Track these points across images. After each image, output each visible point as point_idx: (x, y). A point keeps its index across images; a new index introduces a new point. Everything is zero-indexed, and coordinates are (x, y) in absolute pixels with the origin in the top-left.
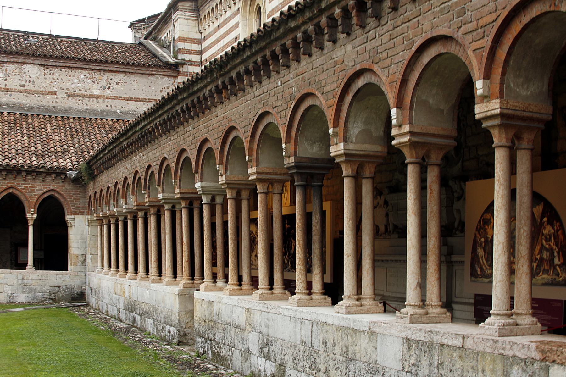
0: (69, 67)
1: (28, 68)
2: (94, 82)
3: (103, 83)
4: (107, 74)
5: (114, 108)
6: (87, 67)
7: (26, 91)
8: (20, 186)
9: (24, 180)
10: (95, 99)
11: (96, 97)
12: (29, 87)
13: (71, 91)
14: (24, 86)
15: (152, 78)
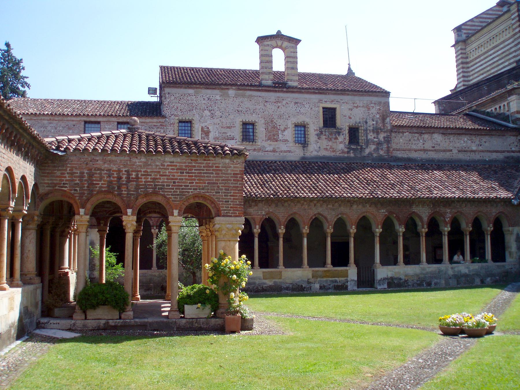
0: (459, 134)
1: (436, 136)
2: (472, 142)
3: (478, 142)
4: (479, 137)
5: (485, 158)
6: (469, 133)
7: (435, 150)
9: (486, 207)
10: (474, 153)
11: (474, 151)
12: (437, 148)
13: (460, 149)
14: (434, 147)
15: (504, 138)
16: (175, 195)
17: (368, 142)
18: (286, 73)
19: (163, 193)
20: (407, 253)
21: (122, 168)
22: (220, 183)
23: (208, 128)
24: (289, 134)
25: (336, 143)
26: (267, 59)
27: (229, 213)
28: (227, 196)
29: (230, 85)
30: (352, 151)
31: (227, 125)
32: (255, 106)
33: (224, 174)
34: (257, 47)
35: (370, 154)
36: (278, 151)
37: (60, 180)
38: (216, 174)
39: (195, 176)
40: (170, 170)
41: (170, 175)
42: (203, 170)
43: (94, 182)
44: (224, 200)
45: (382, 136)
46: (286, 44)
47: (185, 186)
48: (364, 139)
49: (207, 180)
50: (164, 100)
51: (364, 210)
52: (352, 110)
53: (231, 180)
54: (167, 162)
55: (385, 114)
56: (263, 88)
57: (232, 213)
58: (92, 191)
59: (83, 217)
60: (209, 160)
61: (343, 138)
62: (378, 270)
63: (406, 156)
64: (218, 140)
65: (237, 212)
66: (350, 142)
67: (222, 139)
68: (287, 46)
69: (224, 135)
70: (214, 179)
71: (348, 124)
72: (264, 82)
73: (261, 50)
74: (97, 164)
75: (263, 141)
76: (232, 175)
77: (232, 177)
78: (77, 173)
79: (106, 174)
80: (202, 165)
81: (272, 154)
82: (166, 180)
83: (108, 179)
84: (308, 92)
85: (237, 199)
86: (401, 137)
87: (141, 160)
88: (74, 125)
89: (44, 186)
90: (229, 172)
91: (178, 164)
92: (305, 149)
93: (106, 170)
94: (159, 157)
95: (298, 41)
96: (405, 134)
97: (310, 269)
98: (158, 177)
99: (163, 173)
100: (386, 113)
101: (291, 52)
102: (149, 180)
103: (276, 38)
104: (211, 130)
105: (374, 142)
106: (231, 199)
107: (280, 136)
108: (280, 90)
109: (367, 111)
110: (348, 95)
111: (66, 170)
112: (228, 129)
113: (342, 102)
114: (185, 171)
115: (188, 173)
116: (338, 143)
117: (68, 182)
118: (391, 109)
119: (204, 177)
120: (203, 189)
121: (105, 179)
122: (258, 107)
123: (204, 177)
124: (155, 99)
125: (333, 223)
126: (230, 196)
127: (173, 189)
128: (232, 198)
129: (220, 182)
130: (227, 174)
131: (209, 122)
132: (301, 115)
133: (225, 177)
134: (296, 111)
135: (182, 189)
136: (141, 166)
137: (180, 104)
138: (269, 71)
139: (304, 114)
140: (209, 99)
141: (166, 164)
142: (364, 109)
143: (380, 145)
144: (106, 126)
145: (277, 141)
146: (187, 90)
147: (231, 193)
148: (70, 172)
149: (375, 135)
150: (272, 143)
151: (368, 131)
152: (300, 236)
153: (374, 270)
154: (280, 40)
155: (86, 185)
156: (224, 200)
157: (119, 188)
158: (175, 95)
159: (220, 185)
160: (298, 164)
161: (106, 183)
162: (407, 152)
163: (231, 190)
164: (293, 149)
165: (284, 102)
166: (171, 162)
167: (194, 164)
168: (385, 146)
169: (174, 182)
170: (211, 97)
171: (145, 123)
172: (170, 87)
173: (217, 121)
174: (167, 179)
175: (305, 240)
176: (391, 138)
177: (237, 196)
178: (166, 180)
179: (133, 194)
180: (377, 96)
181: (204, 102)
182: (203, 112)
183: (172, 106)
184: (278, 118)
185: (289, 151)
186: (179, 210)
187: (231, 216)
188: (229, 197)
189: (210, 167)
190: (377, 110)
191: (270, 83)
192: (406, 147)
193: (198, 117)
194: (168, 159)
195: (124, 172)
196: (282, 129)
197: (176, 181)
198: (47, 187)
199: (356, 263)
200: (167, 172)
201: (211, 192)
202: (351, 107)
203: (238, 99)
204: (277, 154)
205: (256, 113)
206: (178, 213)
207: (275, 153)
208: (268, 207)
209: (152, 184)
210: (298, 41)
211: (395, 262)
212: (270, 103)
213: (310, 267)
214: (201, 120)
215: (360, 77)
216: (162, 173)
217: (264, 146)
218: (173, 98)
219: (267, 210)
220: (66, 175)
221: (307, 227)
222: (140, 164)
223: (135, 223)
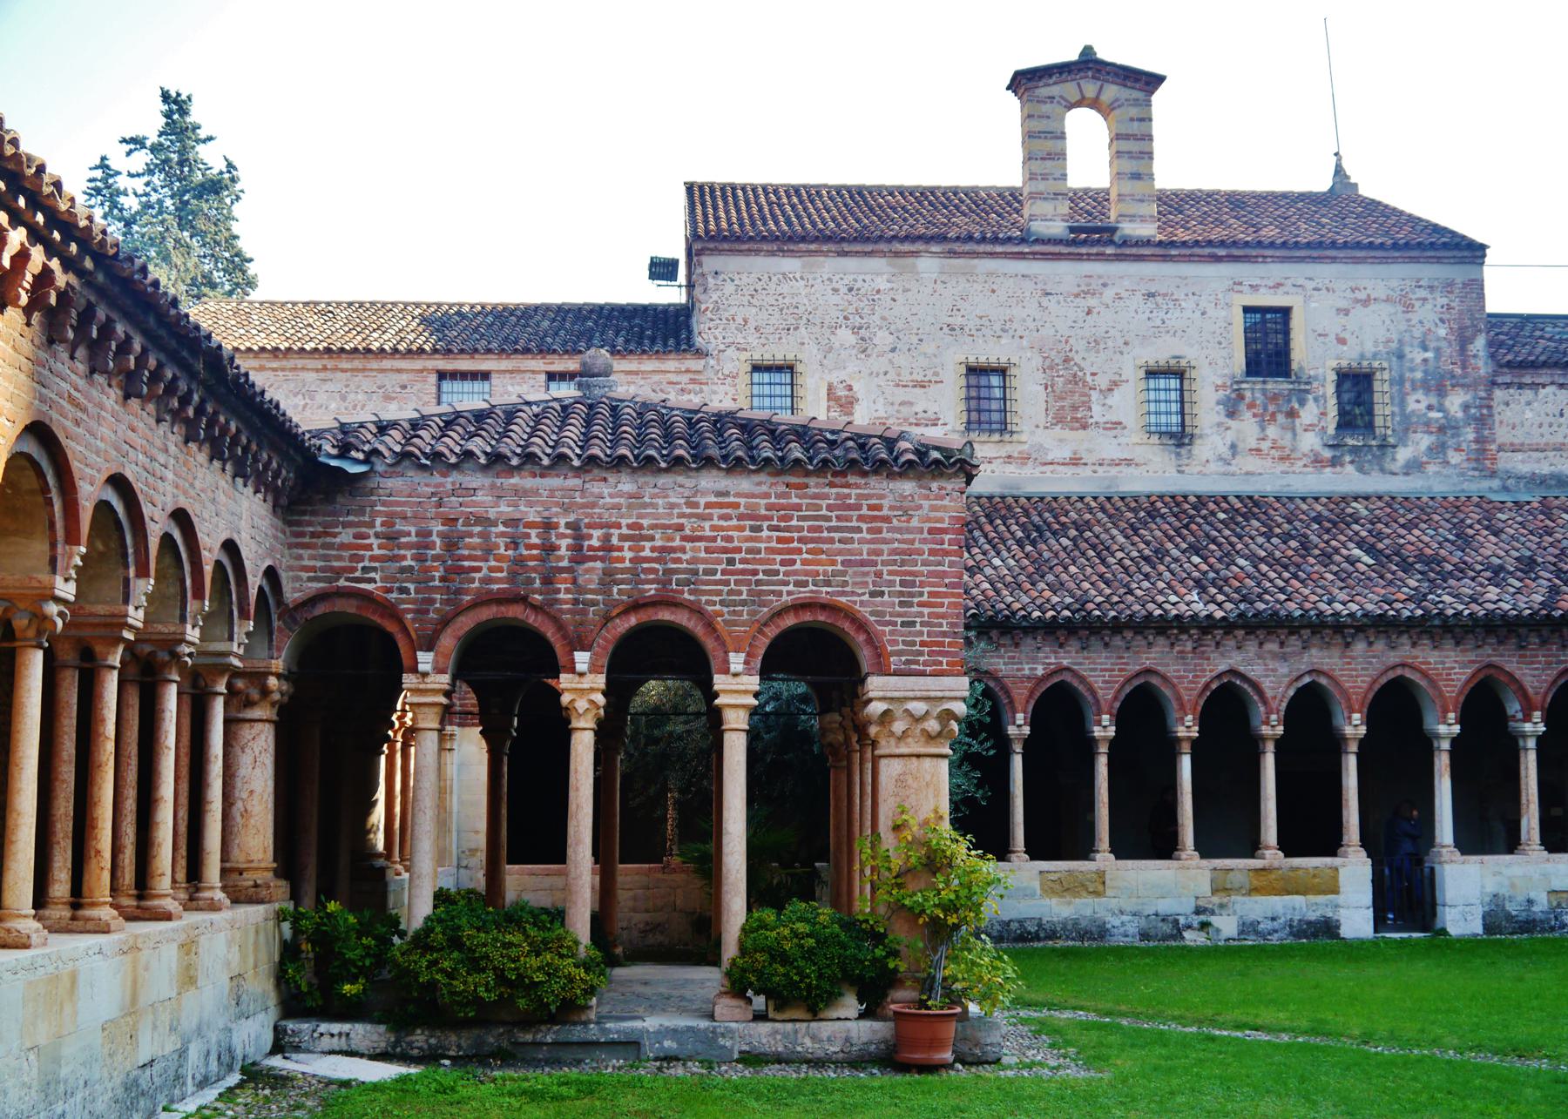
16: (734, 603)
17: (1407, 425)
18: (1113, 196)
19: (692, 598)
20: (1556, 812)
21: (557, 515)
22: (884, 563)
23: (850, 388)
24: (1127, 404)
25: (1293, 430)
26: (1049, 145)
27: (917, 663)
28: (911, 605)
29: (920, 238)
30: (1348, 458)
31: (915, 377)
32: (1008, 311)
33: (899, 530)
34: (1013, 103)
35: (1415, 466)
36: (1090, 461)
37: (352, 556)
38: (870, 531)
39: (800, 540)
40: (716, 522)
41: (715, 537)
42: (828, 519)
43: (466, 564)
44: (899, 620)
45: (1455, 402)
46: (1111, 92)
47: (765, 572)
48: (1393, 414)
49: (840, 553)
50: (702, 297)
51: (1393, 657)
52: (1346, 312)
53: (920, 552)
54: (704, 494)
55: (1468, 323)
56: (1037, 248)
57: (925, 663)
58: (458, 592)
59: (428, 680)
60: (848, 486)
61: (1316, 411)
62: (1447, 867)
63: (1545, 469)
65: (945, 660)
66: (1346, 423)
68: (1117, 100)
70: (865, 547)
71: (1334, 364)
72: (1039, 228)
73: (1028, 117)
74: (475, 504)
75: (1037, 426)
76: (925, 535)
77: (924, 541)
78: (409, 534)
79: (503, 534)
80: (824, 503)
81: (1070, 470)
82: (703, 555)
83: (510, 552)
84: (1190, 255)
85: (943, 616)
86: (1529, 403)
87: (620, 487)
88: (404, 387)
89: (298, 579)
90: (915, 523)
91: (742, 501)
92: (1183, 451)
93: (505, 524)
94: (681, 479)
95: (1152, 81)
96: (1542, 392)
97: (1205, 862)
98: (677, 543)
99: (693, 530)
100: (1472, 318)
101: (1132, 120)
102: (647, 553)
103: (1080, 70)
104: (859, 395)
105: (1428, 424)
106: (921, 614)
107: (1096, 409)
108: (1094, 250)
109: (1400, 316)
110: (1334, 260)
111: (371, 525)
112: (918, 391)
113: (1310, 285)
114: (765, 524)
115: (776, 528)
116: (1299, 430)
117: (377, 564)
118: (1493, 306)
119: (831, 541)
120: (828, 583)
121: (502, 551)
122: (1017, 312)
123: (831, 541)
124: (670, 294)
125: (1284, 705)
126: (920, 604)
127: (727, 583)
128: (926, 610)
129: (885, 558)
130: (908, 531)
131: (850, 369)
132: (1167, 337)
133: (900, 542)
134: (1151, 324)
135: (758, 583)
136: (618, 507)
137: (754, 310)
138: (1058, 187)
139: (1179, 333)
140: (851, 290)
141: (702, 501)
142: (1389, 308)
143: (1450, 433)
144: (510, 388)
145: (1084, 427)
146: (775, 259)
147: (921, 594)
148: (384, 529)
149: (1433, 400)
150: (1067, 434)
151: (1408, 385)
152: (1170, 748)
153: (1432, 869)
154: (1093, 77)
155: (437, 574)
156: (899, 620)
157: (548, 581)
158: (736, 277)
159: (885, 569)
160: (1159, 504)
161: (505, 565)
162: (1551, 454)
163: (922, 584)
164: (1139, 453)
165: (1109, 294)
166: (719, 494)
167: (795, 500)
168: (1469, 434)
169: (731, 562)
171: (636, 373)
172: (720, 252)
174: (707, 550)
175: (1186, 765)
176: (1490, 407)
177: (942, 605)
178: (703, 555)
179: (594, 603)
180: (1439, 260)
181: (836, 299)
182: (833, 333)
183: (727, 315)
184: (1087, 350)
185: (1129, 462)
186: (749, 655)
187: (922, 674)
188: (916, 609)
189: (850, 507)
190: (1438, 308)
191: (1058, 228)
192: (1548, 438)
194: (710, 482)
195: (562, 530)
196: (1104, 387)
197: (737, 556)
198: (310, 579)
199: (1366, 842)
200: (707, 528)
201: (853, 593)
202: (1343, 304)
203: (948, 285)
204: (1086, 472)
205: (1011, 332)
206: (746, 663)
207: (1079, 470)
208: (1055, 652)
209: (657, 566)
210: (1152, 81)
211: (1512, 844)
212: (1061, 298)
213: (1203, 856)
214: (825, 362)
215: (1378, 198)
216: (687, 532)
217: (1041, 445)
218: (729, 288)
219: (1053, 661)
220: (372, 540)
221: (1190, 717)
222: (616, 500)
223: (600, 699)
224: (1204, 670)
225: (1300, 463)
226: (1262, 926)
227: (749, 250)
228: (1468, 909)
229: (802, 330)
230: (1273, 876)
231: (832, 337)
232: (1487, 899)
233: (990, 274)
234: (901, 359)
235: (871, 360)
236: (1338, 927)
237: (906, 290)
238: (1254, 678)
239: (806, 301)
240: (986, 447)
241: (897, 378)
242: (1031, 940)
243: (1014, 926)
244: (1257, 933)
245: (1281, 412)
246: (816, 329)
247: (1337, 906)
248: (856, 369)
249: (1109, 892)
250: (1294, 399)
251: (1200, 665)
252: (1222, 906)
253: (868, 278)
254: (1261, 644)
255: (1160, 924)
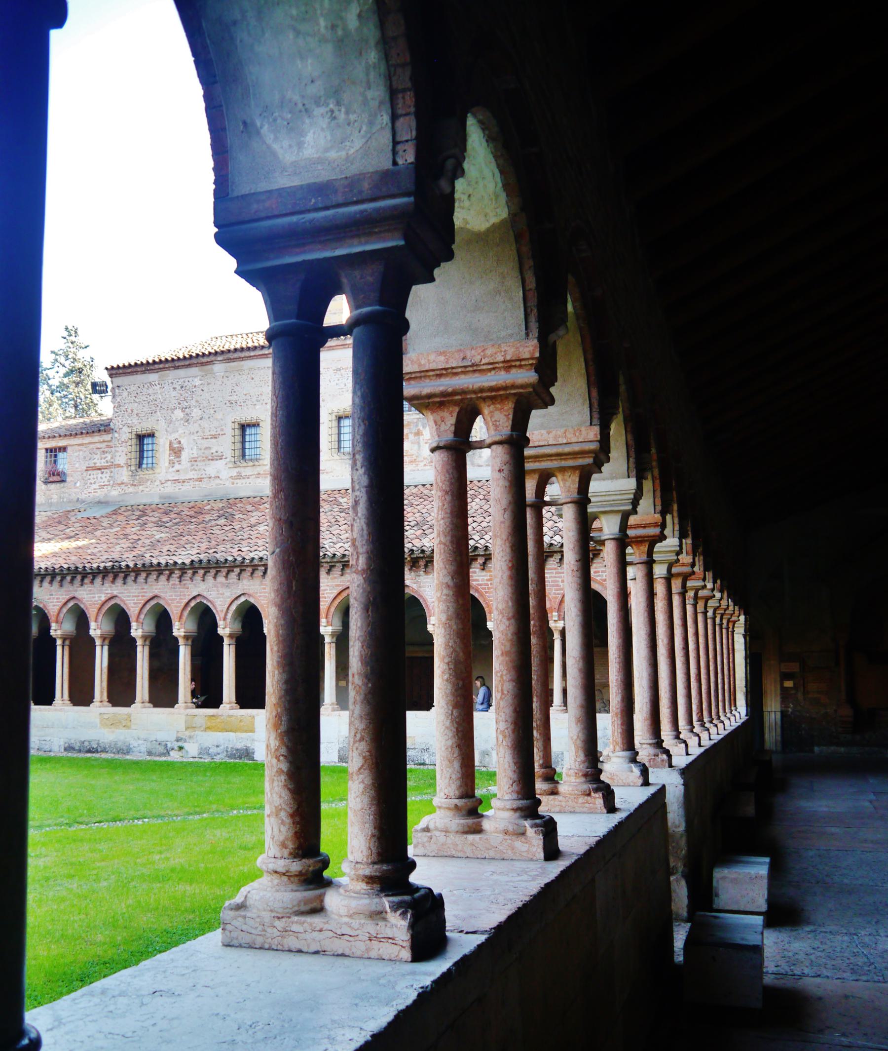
8: (599, 576)
23: (180, 442)
25: (419, 443)
64: (195, 463)
67: (204, 461)
69: (206, 452)
104: (185, 446)
112: (214, 440)
131: (180, 432)
137: (136, 404)
140: (182, 387)
158: (128, 388)
170: (185, 384)
173: (194, 427)
181: (174, 393)
182: (173, 413)
183: (123, 409)
193: (163, 424)
203: (230, 378)
205: (261, 401)
208: (111, 587)
219: (110, 592)
224: (184, 595)
225: (422, 464)
226: (211, 750)
227: (132, 372)
228: (329, 745)
229: (158, 413)
230: (218, 720)
231: (172, 415)
232: (342, 740)
233: (250, 369)
234: (205, 424)
235: (190, 426)
236: (253, 753)
237: (209, 384)
238: (211, 599)
239: (160, 397)
240: (247, 469)
241: (202, 434)
242: (94, 752)
243: (86, 744)
244: (208, 754)
245: (411, 433)
246: (164, 412)
247: (253, 740)
248: (183, 431)
249: (133, 727)
250: (420, 424)
251: (184, 592)
252: (190, 737)
253: (190, 379)
254: (215, 577)
255: (158, 746)
